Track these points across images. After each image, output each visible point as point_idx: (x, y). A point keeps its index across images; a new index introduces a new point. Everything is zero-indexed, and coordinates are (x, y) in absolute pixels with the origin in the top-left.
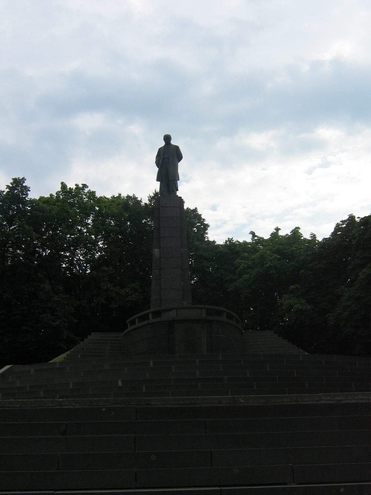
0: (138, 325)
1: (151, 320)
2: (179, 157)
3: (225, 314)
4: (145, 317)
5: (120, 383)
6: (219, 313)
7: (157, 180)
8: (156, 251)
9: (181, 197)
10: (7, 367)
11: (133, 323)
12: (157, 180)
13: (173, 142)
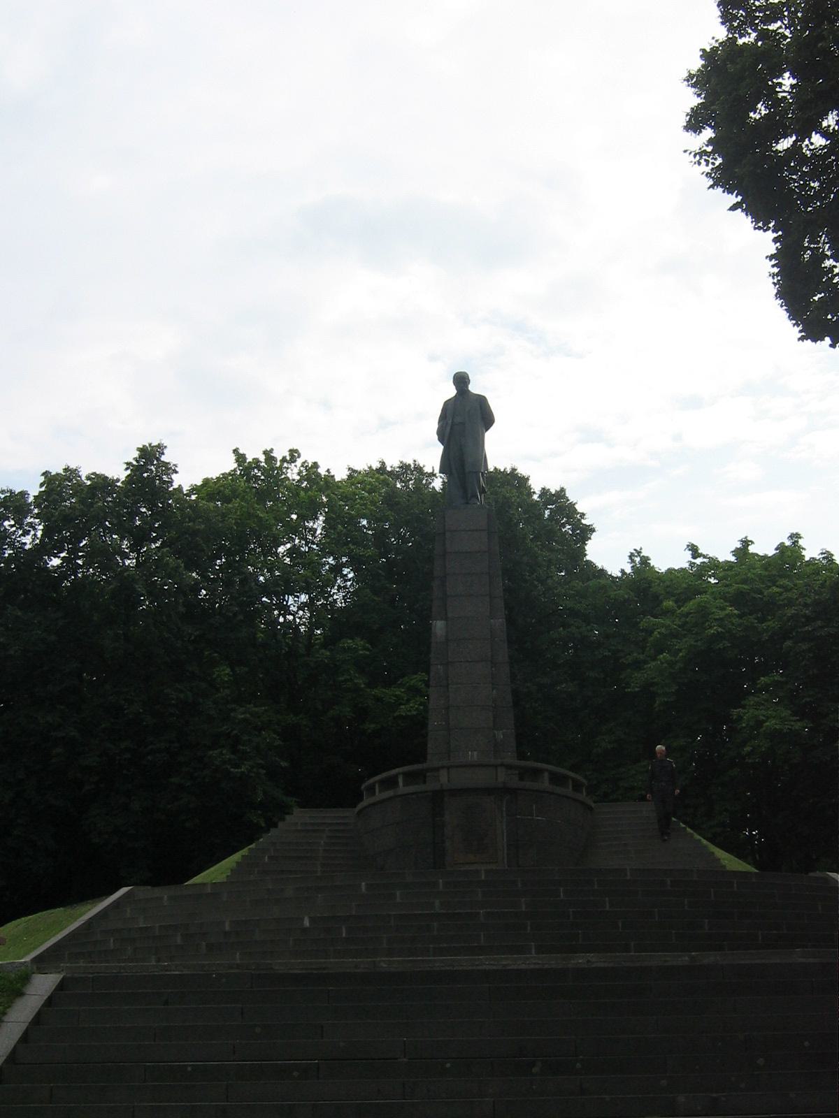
0: (380, 795)
1: (402, 788)
2: (487, 419)
3: (546, 775)
4: (391, 783)
5: (307, 923)
6: (536, 773)
8: (439, 626)
10: (124, 890)
11: (371, 789)
13: (474, 388)
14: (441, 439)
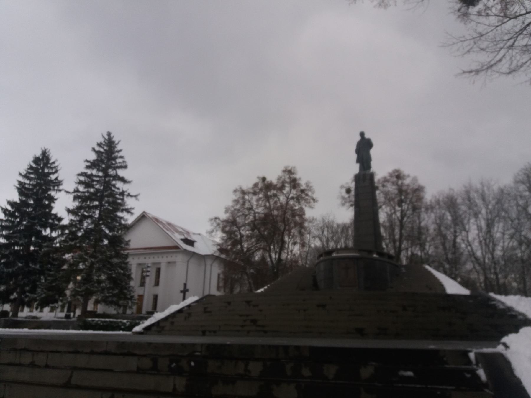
13: (367, 136)
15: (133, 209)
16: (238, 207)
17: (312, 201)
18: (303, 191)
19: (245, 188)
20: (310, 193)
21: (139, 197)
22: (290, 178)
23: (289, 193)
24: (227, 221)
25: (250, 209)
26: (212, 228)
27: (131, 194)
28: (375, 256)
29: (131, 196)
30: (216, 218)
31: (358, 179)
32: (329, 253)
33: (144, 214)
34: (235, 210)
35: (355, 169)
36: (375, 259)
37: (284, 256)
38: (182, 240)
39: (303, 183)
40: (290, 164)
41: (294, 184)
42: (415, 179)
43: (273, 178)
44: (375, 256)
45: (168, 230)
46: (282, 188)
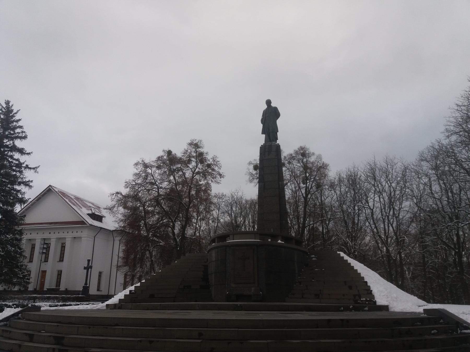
7: (262, 134)
9: (279, 144)
12: (262, 134)
13: (273, 105)
14: (262, 123)
15: (32, 181)
16: (139, 181)
17: (219, 177)
18: (209, 166)
19: (147, 161)
20: (216, 168)
21: (38, 170)
22: (196, 152)
23: (195, 167)
24: (126, 197)
25: (152, 184)
26: (114, 203)
27: (29, 166)
28: (279, 241)
29: (30, 168)
30: (118, 193)
31: (264, 150)
32: (223, 238)
33: (50, 187)
34: (136, 184)
35: (261, 139)
36: (280, 246)
37: (189, 232)
38: (88, 214)
39: (209, 157)
40: (197, 138)
41: (201, 157)
42: (319, 157)
43: (178, 152)
44: (279, 241)
45: (74, 205)
46: (189, 161)
